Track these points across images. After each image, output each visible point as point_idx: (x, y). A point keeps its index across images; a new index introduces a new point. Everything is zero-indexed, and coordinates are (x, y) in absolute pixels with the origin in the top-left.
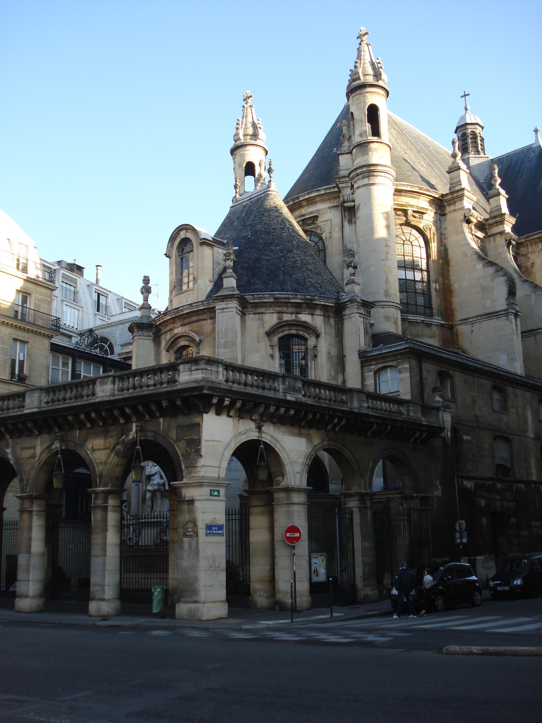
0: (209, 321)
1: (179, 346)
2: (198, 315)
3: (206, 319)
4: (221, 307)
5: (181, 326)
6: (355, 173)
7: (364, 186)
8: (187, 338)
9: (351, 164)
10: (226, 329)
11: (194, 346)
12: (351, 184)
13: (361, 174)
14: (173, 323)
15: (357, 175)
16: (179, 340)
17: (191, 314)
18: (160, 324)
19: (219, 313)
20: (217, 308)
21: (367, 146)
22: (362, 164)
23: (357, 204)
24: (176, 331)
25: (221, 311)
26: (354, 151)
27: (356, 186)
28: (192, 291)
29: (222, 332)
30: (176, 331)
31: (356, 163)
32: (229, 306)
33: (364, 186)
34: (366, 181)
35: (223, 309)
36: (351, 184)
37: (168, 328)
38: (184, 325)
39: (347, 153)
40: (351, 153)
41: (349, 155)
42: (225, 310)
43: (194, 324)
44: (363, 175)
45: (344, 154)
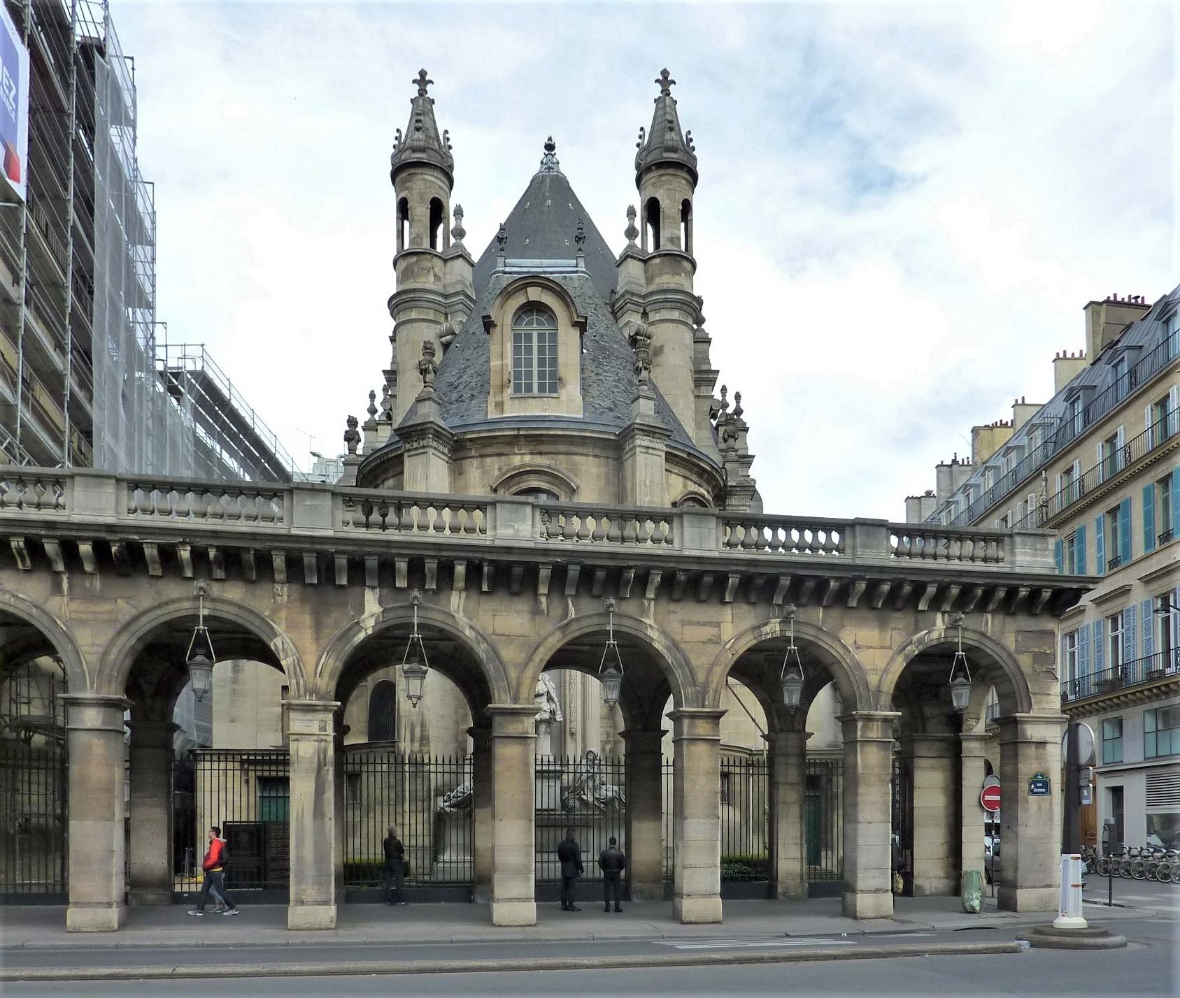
0: (591, 459)
1: (524, 486)
2: (571, 444)
3: (588, 455)
4: (645, 443)
5: (532, 454)
6: (663, 297)
7: (672, 321)
8: (544, 477)
9: (643, 281)
10: (652, 482)
11: (563, 494)
12: (645, 310)
13: (671, 302)
14: (509, 444)
15: (666, 300)
16: (524, 476)
17: (559, 439)
18: (471, 440)
19: (641, 452)
20: (638, 442)
21: (680, 261)
22: (672, 286)
23: (656, 342)
24: (516, 460)
25: (644, 450)
26: (657, 261)
27: (653, 317)
28: (556, 400)
29: (645, 485)
30: (516, 460)
31: (658, 281)
32: (657, 446)
33: (672, 321)
34: (676, 315)
35: (647, 447)
36: (645, 310)
37: (490, 450)
38: (540, 453)
39: (640, 260)
40: (645, 262)
41: (640, 264)
42: (650, 451)
43: (562, 457)
44: (673, 304)
45: (634, 258)
